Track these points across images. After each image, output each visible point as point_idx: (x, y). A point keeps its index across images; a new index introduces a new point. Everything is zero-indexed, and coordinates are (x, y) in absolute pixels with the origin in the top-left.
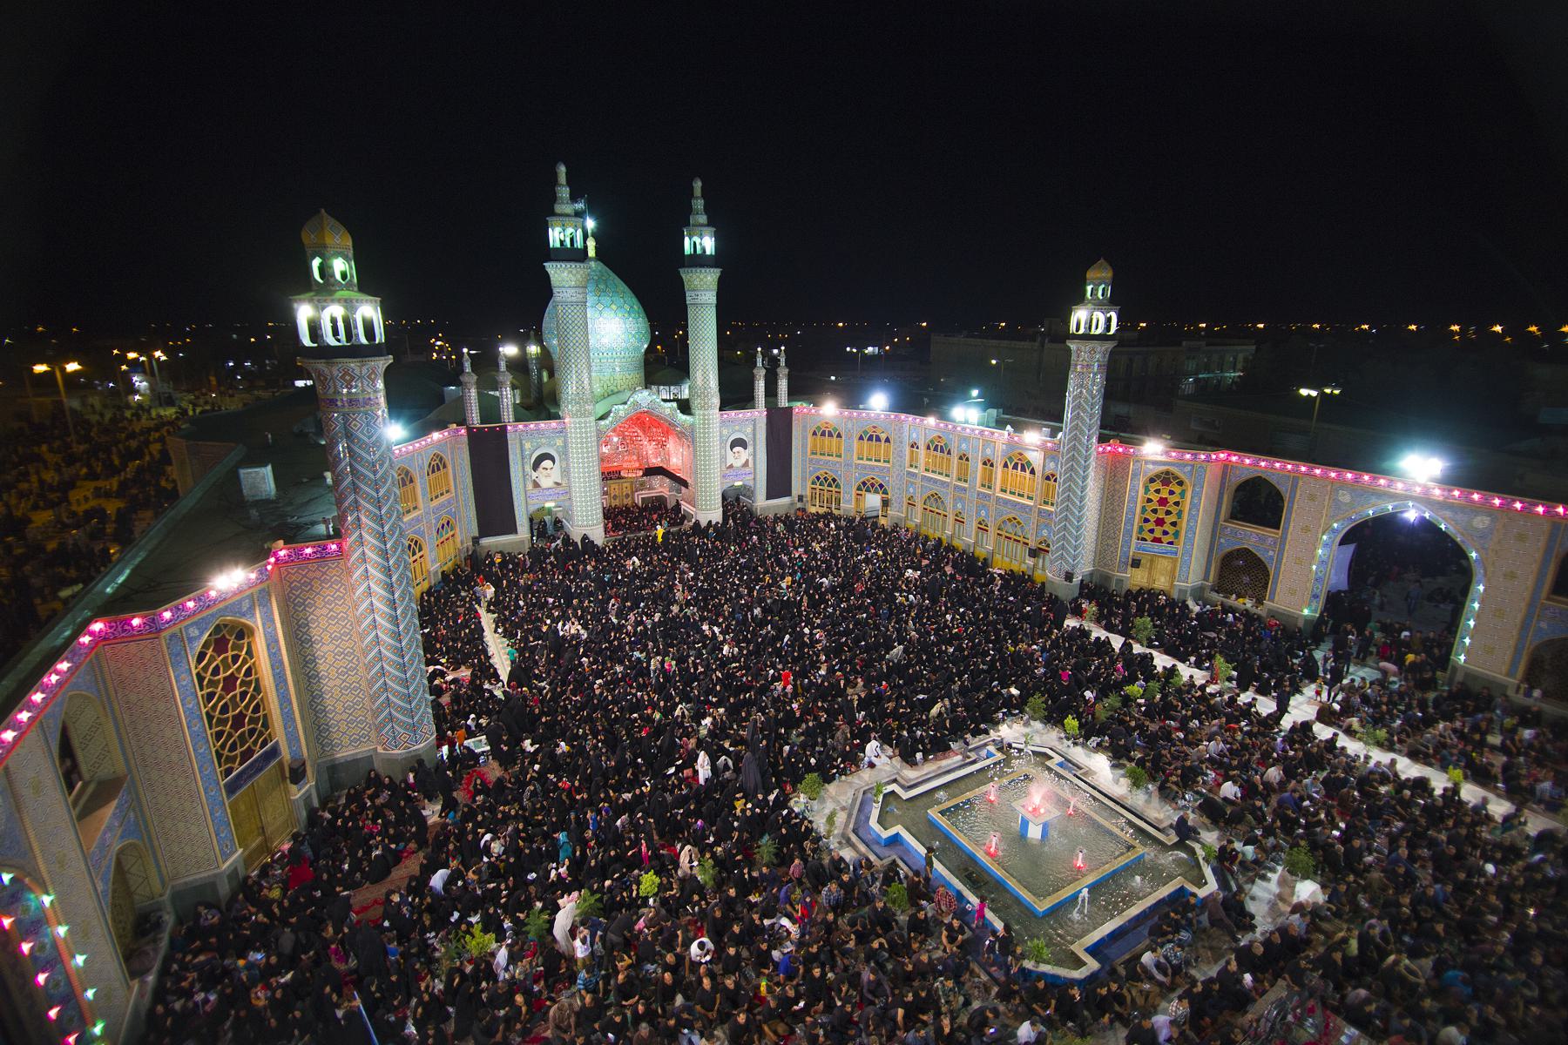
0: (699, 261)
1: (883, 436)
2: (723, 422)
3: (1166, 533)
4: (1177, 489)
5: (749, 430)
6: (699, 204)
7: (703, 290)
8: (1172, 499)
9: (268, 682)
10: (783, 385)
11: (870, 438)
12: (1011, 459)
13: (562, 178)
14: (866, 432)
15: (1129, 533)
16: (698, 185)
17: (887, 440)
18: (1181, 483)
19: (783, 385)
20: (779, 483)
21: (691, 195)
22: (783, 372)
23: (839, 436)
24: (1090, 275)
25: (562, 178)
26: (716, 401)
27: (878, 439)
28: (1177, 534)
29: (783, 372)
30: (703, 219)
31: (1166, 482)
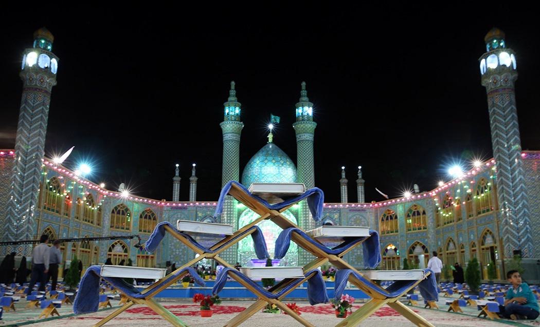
0: (303, 118)
1: (421, 210)
5: (336, 216)
7: (306, 134)
10: (361, 189)
11: (414, 214)
12: (479, 187)
13: (233, 87)
14: (410, 210)
16: (304, 84)
17: (424, 213)
19: (361, 189)
21: (300, 89)
22: (360, 181)
23: (396, 217)
25: (233, 87)
27: (419, 214)
29: (360, 181)
30: (306, 99)
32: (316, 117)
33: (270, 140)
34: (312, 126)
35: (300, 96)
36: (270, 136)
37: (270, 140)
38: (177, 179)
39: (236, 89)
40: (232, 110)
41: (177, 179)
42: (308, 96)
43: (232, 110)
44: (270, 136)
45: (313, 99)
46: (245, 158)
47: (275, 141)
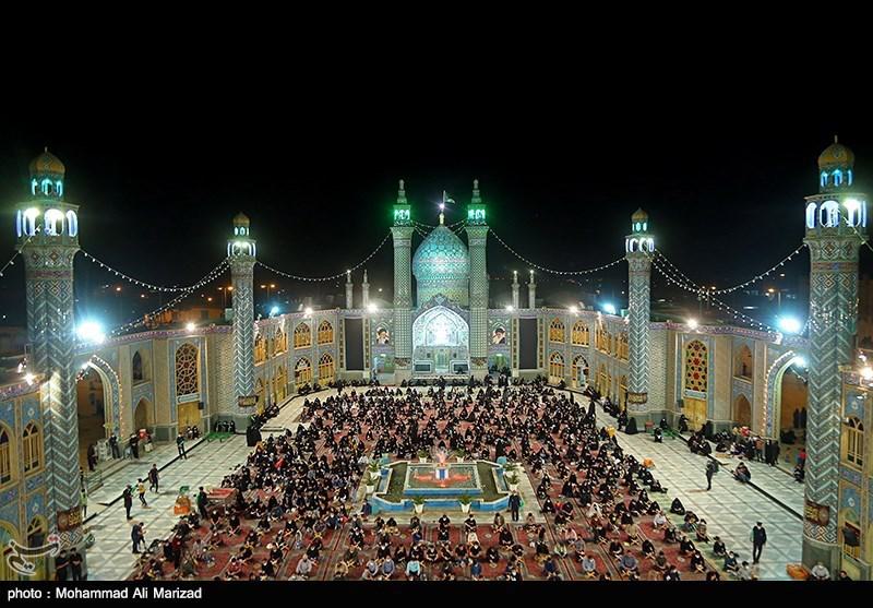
2: (489, 317)
3: (700, 384)
4: (703, 353)
6: (476, 192)
8: (702, 359)
9: (199, 370)
10: (532, 294)
13: (402, 187)
15: (679, 383)
16: (476, 182)
18: (704, 349)
20: (528, 360)
22: (532, 286)
24: (634, 217)
26: (485, 302)
28: (705, 384)
30: (478, 200)
31: (697, 348)
32: (489, 221)
33: (442, 222)
34: (483, 231)
35: (471, 195)
36: (442, 217)
37: (442, 222)
38: (349, 286)
39: (405, 189)
40: (402, 213)
41: (349, 286)
42: (481, 196)
43: (402, 213)
44: (442, 217)
45: (486, 199)
46: (416, 243)
47: (446, 224)
